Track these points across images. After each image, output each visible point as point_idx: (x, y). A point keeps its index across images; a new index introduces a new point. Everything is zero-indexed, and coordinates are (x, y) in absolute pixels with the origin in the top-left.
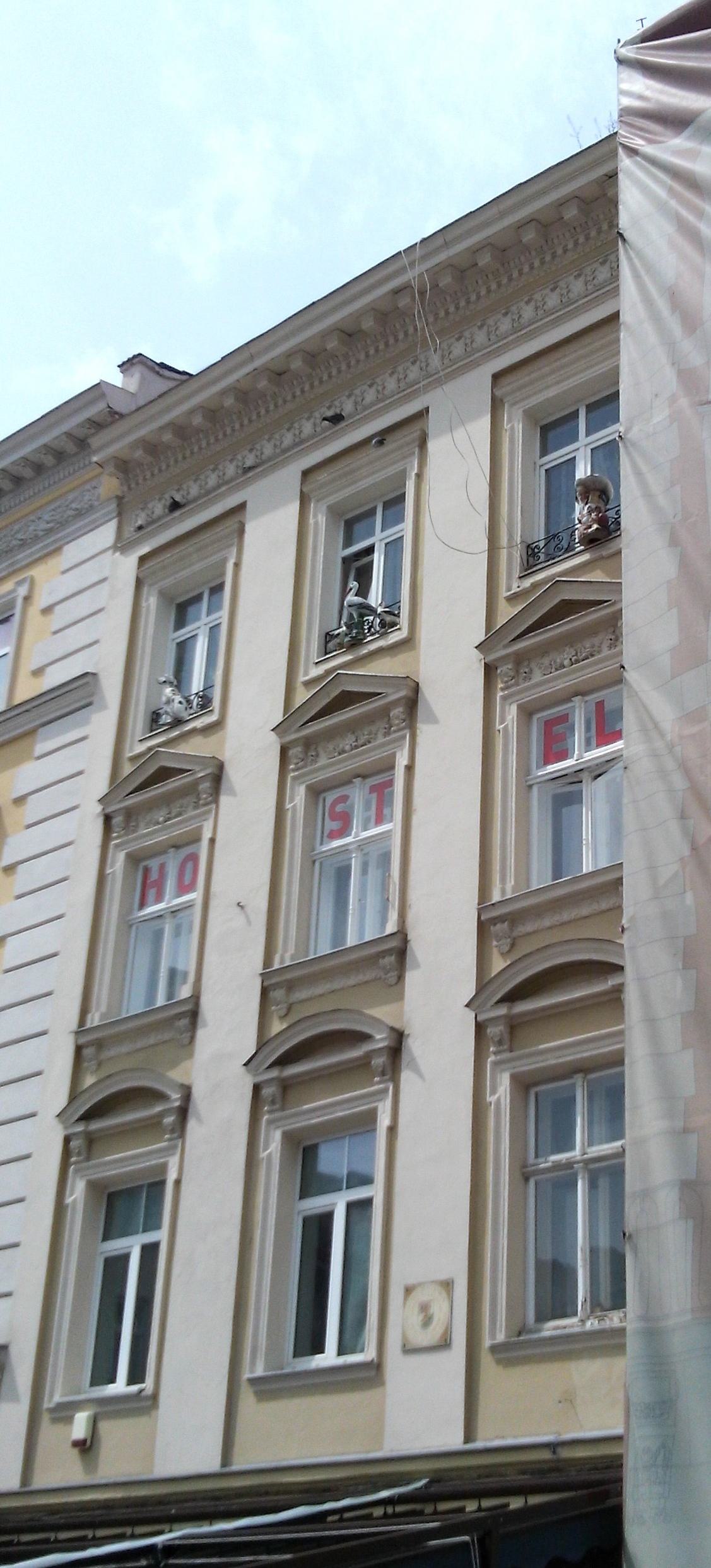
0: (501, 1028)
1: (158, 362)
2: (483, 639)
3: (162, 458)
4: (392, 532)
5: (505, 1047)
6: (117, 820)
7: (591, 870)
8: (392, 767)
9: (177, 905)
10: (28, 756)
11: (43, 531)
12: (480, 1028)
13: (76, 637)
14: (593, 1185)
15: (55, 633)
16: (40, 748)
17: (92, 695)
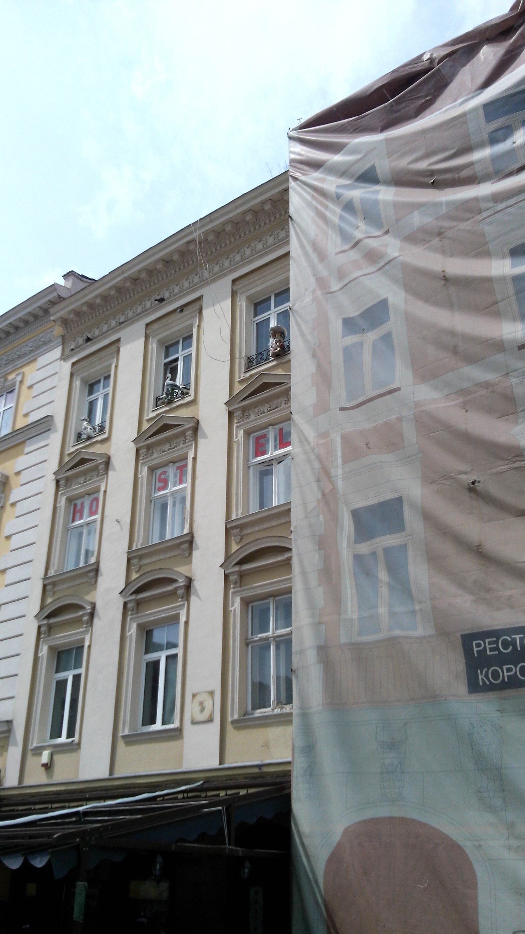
0: (236, 576)
1: (81, 274)
2: (228, 400)
3: (82, 318)
4: (187, 352)
5: (238, 585)
6: (62, 482)
7: (277, 505)
8: (186, 458)
9: (89, 521)
10: (22, 453)
11: (29, 351)
12: (226, 576)
13: (44, 399)
14: (278, 648)
15: (34, 397)
16: (27, 449)
17: (51, 425)
